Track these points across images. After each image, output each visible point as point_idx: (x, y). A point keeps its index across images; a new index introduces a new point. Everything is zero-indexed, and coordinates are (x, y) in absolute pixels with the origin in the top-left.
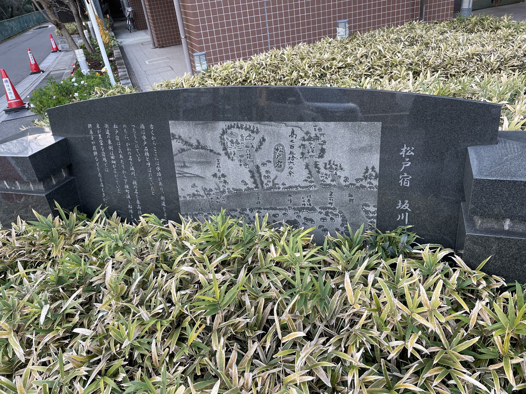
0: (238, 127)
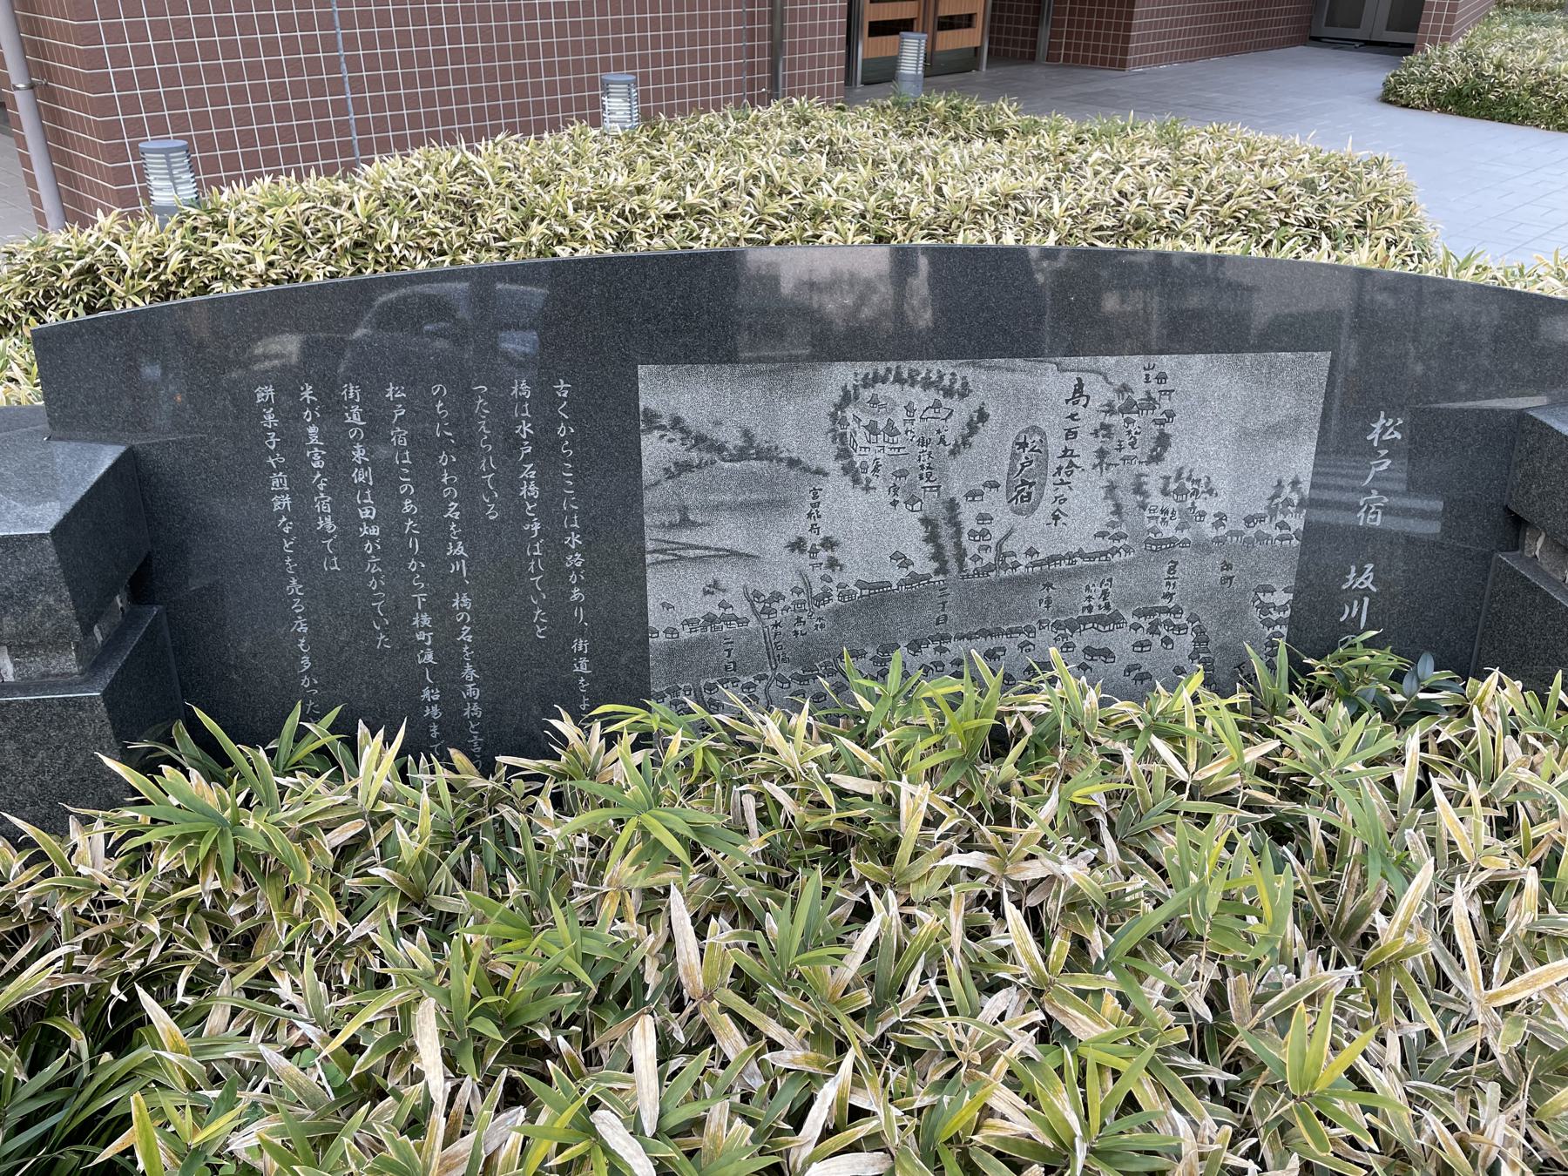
0: (899, 380)
